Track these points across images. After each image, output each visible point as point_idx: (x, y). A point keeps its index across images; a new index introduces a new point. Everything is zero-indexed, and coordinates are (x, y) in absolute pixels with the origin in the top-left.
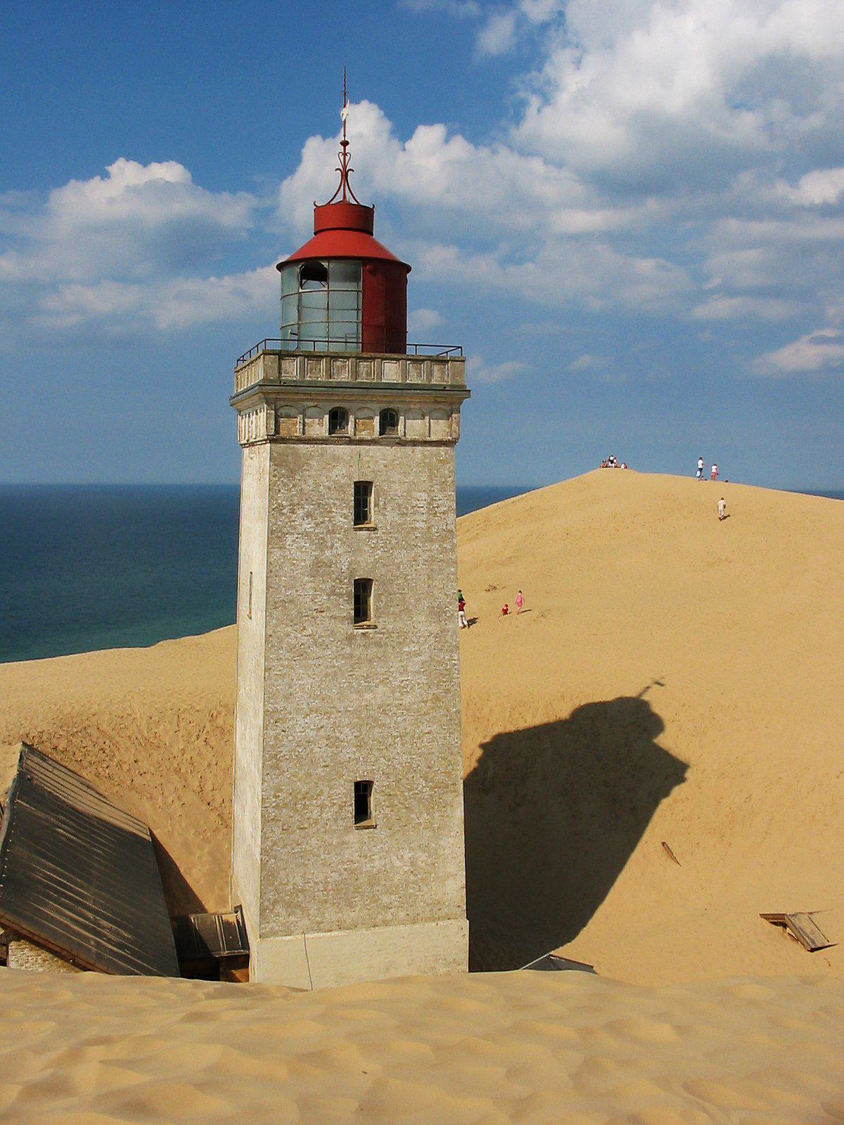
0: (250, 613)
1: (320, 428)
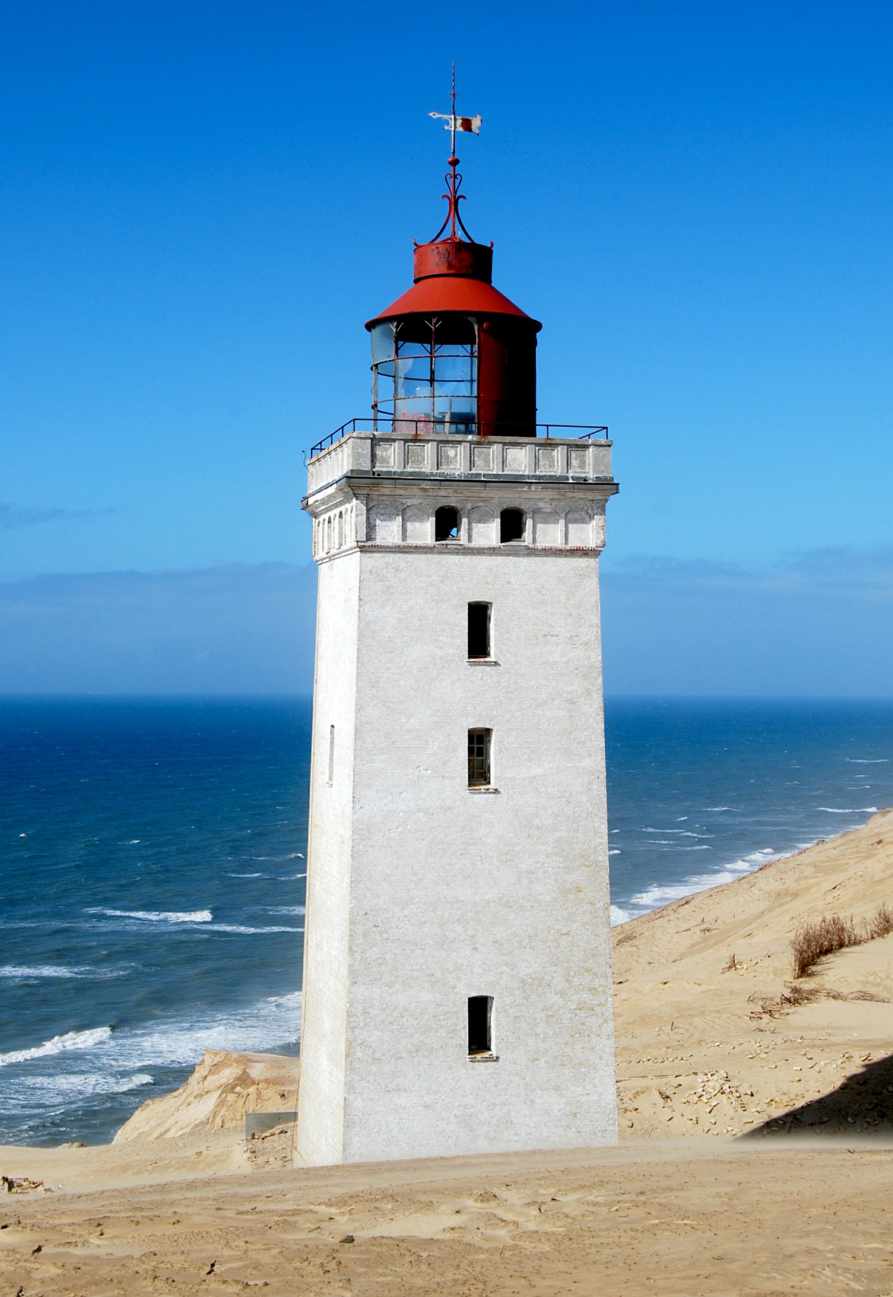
0: (331, 779)
1: (424, 530)
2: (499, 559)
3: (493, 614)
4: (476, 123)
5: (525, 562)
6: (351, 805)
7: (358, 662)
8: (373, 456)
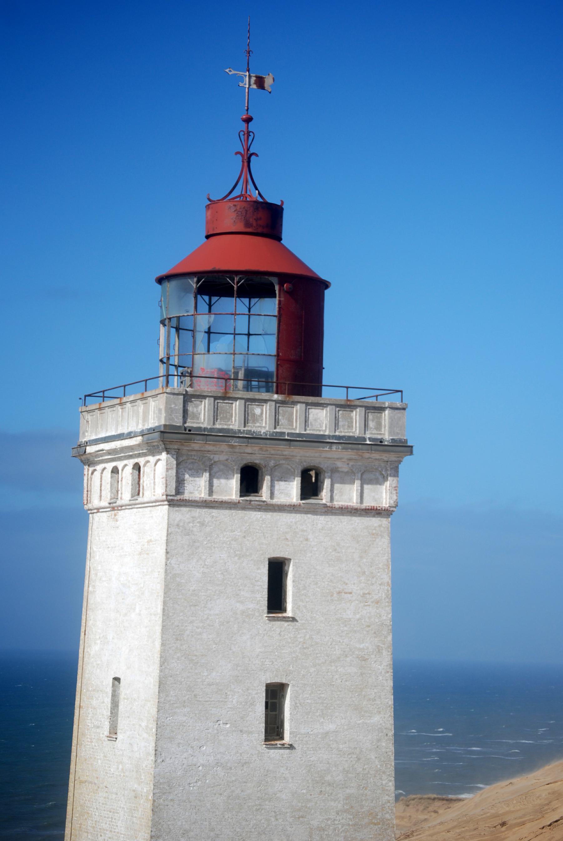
1: (231, 487)
2: (298, 517)
4: (268, 81)
5: (321, 520)
6: (153, 758)
7: (163, 615)
8: (185, 412)
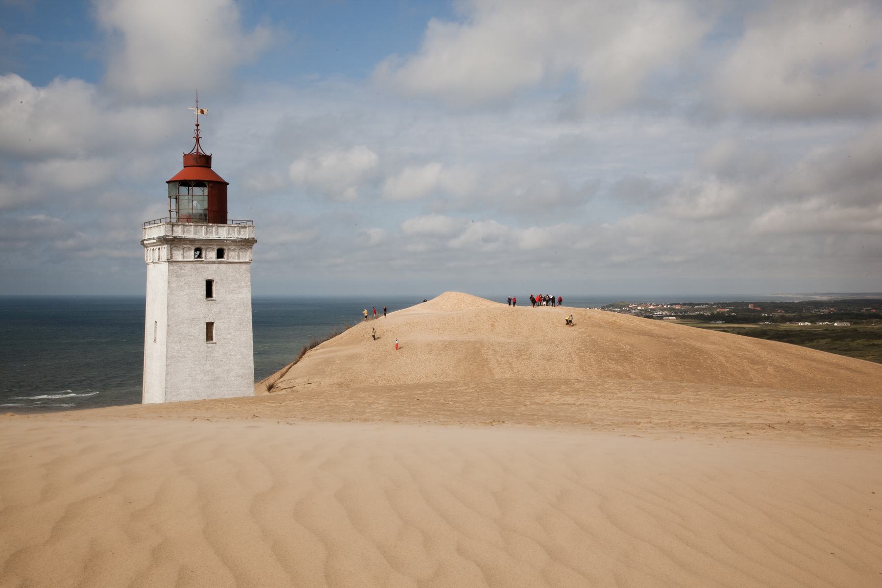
1: (191, 255)
2: (216, 265)
3: (214, 284)
4: (205, 111)
